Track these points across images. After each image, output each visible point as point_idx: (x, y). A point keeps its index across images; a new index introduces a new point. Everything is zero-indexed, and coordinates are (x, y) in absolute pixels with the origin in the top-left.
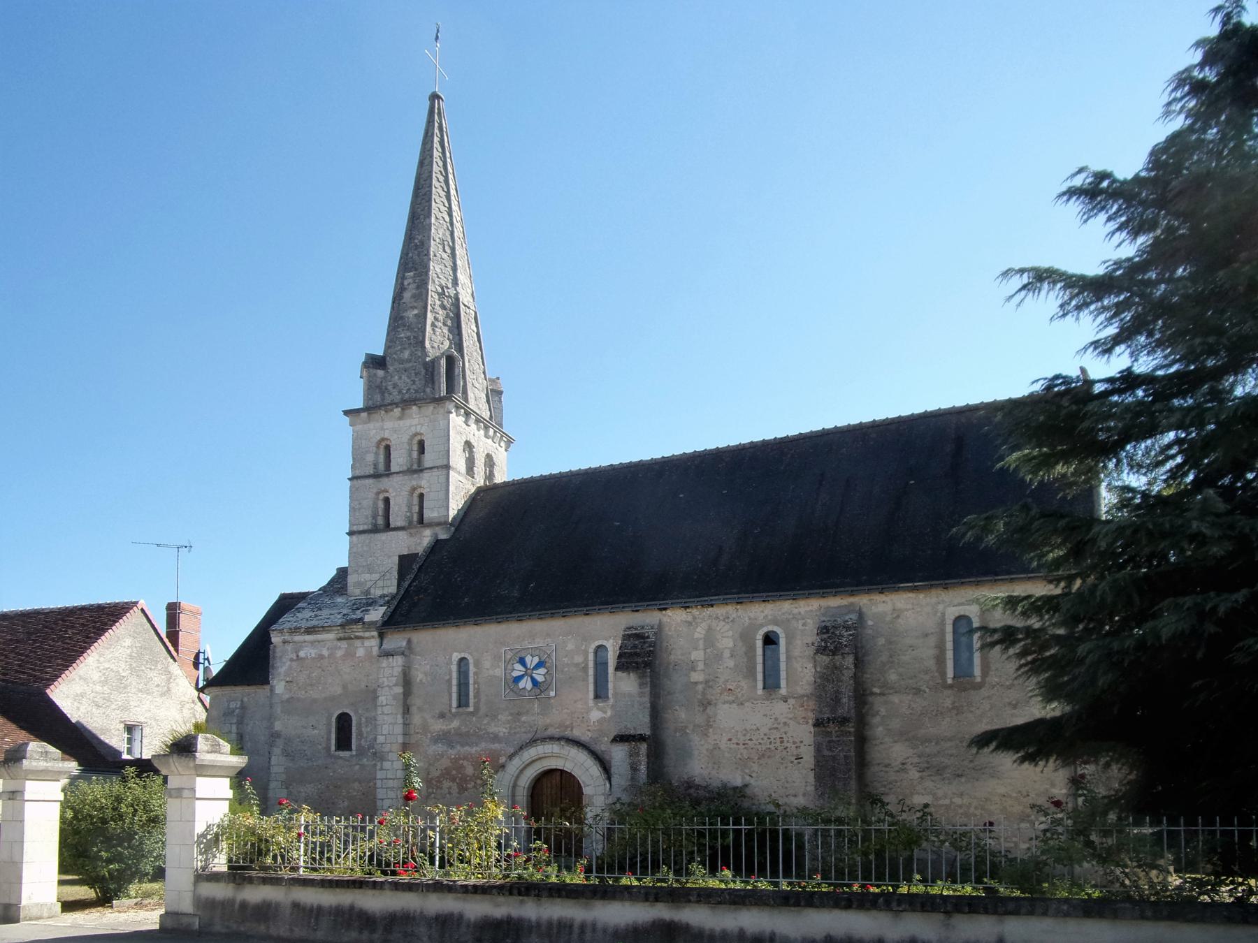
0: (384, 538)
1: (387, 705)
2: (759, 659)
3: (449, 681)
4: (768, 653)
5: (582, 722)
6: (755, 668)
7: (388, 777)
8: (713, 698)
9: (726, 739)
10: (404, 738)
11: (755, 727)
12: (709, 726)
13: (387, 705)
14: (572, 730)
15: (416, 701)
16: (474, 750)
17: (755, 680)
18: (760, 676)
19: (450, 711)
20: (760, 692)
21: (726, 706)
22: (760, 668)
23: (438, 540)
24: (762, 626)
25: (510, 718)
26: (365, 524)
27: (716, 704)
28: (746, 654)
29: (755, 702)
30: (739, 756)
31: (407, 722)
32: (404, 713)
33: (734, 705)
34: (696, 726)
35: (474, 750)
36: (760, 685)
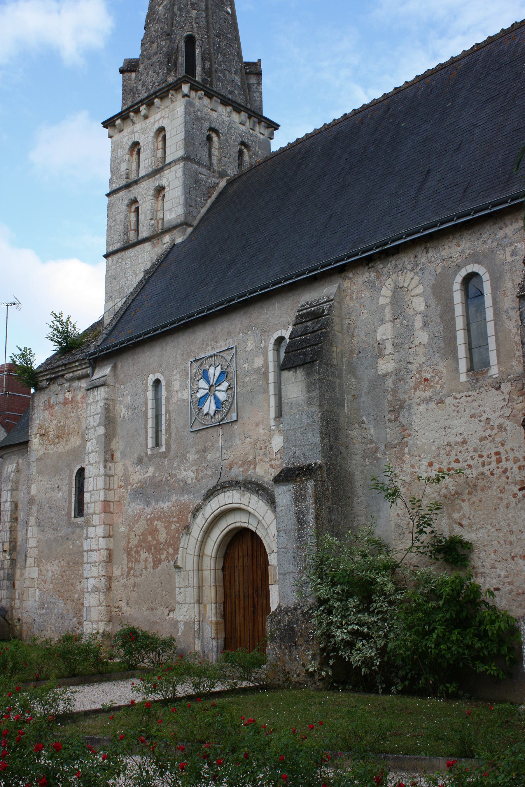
0: (132, 254)
1: (92, 452)
2: (460, 323)
3: (146, 413)
4: (472, 310)
5: (265, 454)
6: (454, 338)
7: (93, 548)
8: (406, 397)
9: (425, 463)
10: (105, 494)
11: (460, 439)
12: (402, 444)
13: (92, 452)
14: (255, 468)
15: (117, 445)
16: (165, 505)
17: (456, 359)
18: (462, 351)
19: (146, 453)
20: (463, 378)
21: (422, 408)
22: (461, 337)
23: (174, 245)
24: (459, 267)
25: (197, 456)
26: (117, 243)
27: (409, 406)
28: (441, 317)
29: (458, 396)
30: (444, 491)
31: (109, 472)
32: (106, 461)
33: (432, 405)
34: (389, 446)
35: (165, 505)
36: (463, 365)
